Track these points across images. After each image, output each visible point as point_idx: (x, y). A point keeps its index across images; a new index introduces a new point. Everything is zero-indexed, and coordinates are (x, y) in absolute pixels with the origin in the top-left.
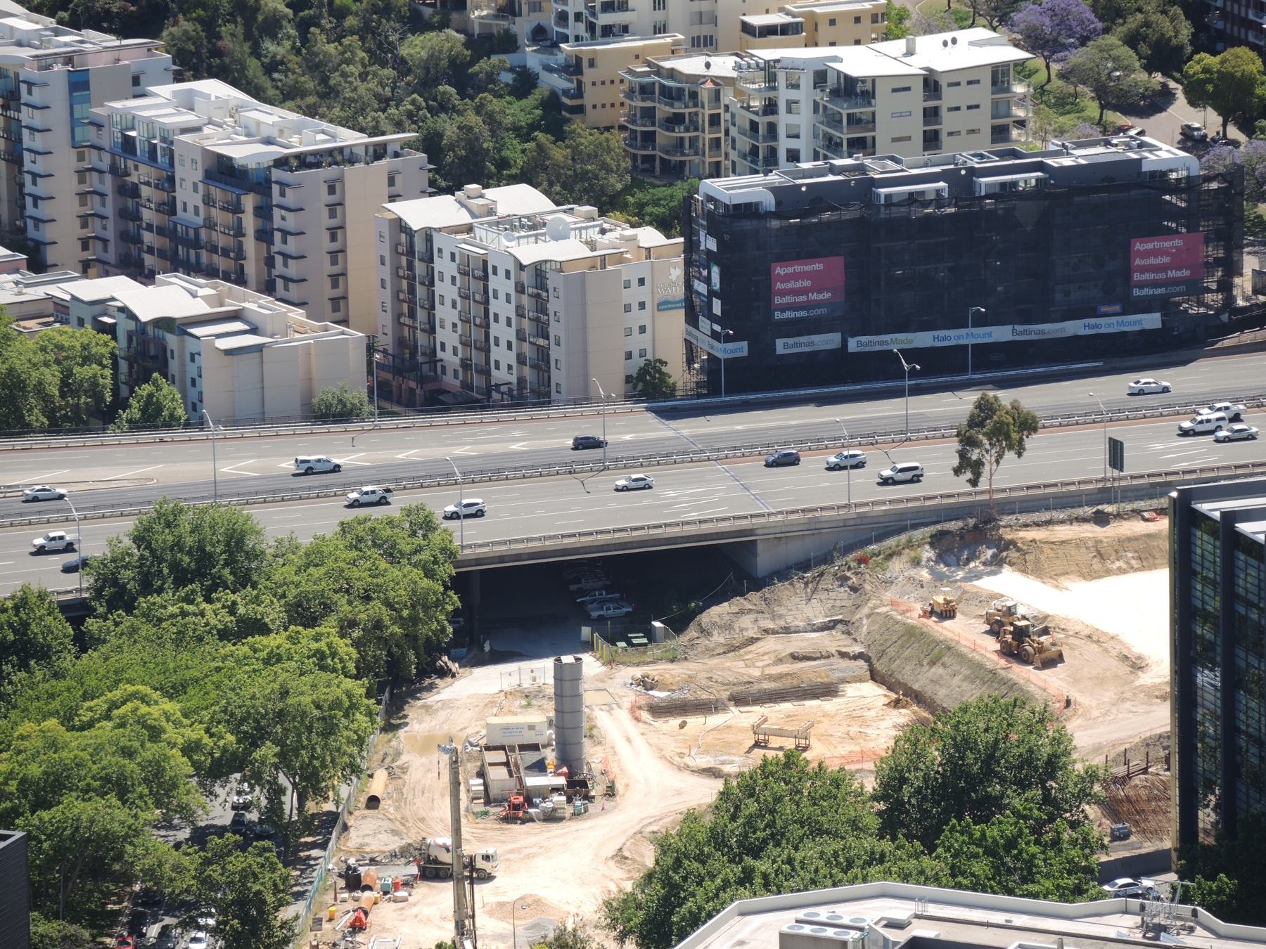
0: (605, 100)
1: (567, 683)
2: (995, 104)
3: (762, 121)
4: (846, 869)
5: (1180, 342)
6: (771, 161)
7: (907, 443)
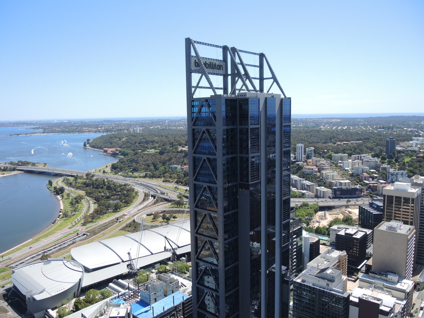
0: (328, 183)
1: (325, 213)
4: (341, 224)
5: (359, 197)
7: (343, 202)
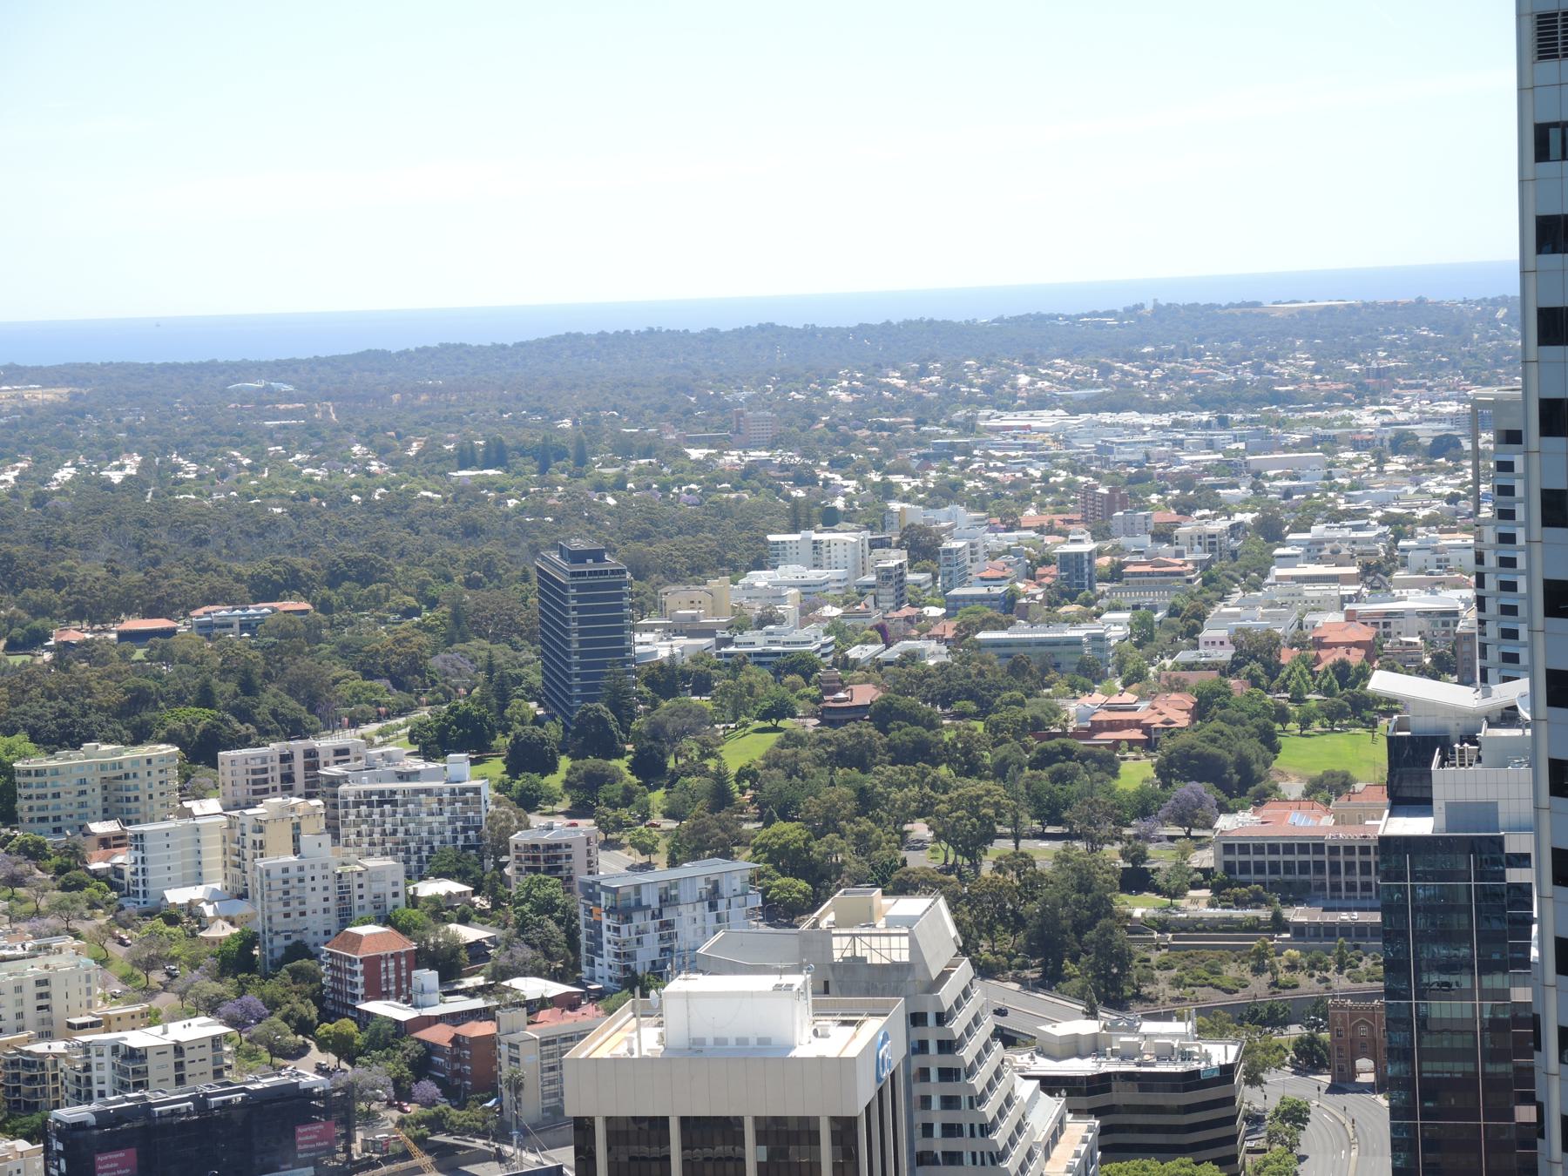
2: (214, 1057)
3: (83, 1076)
6: (89, 1098)
